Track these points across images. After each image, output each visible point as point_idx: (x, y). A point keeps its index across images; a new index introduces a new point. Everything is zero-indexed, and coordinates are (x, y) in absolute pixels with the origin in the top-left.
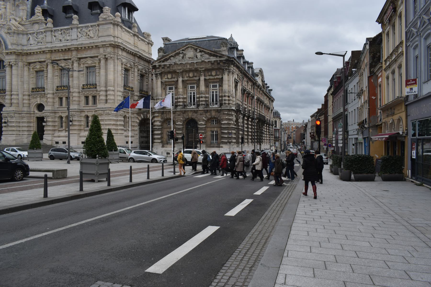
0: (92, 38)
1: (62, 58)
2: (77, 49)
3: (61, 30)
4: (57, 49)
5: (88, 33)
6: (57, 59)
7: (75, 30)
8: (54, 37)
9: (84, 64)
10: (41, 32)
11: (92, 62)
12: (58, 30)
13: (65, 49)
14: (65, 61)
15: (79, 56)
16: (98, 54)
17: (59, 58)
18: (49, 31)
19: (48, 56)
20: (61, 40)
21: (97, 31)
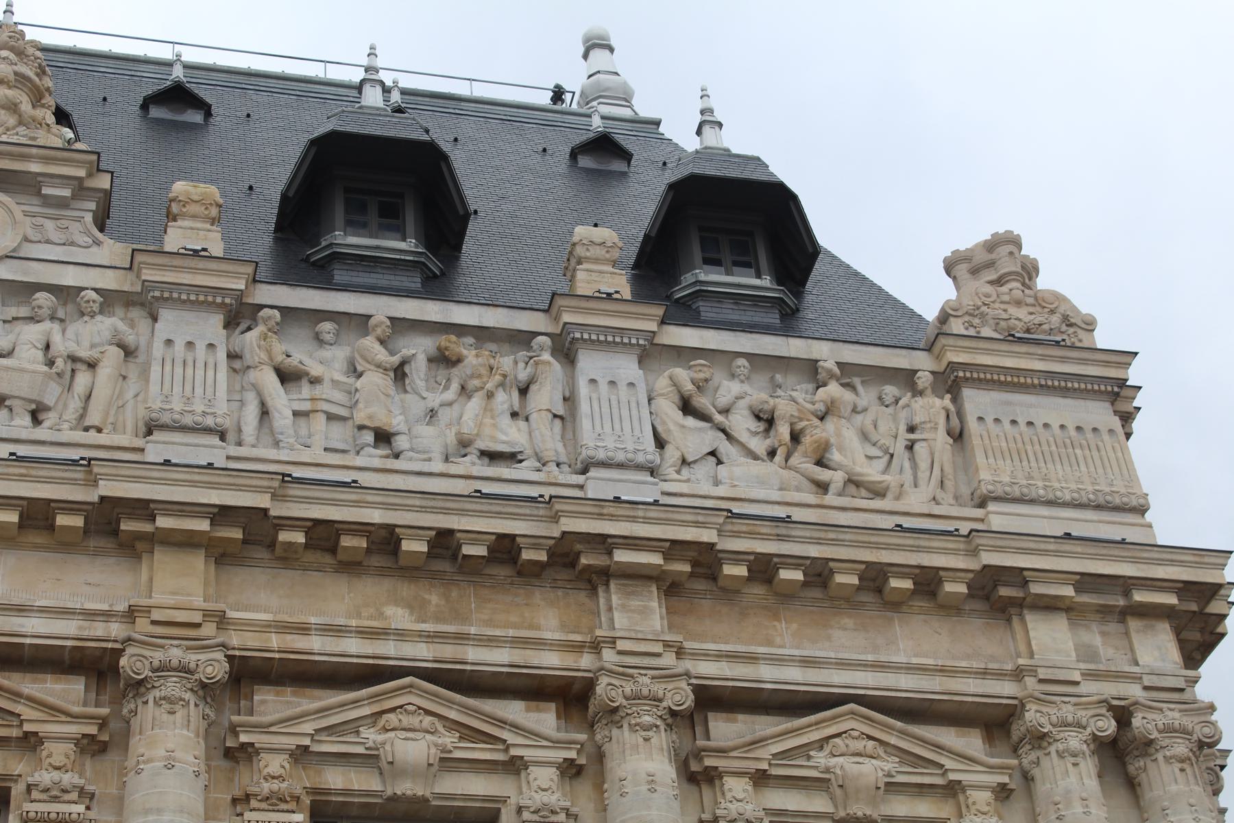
0: (878, 492)
1: (421, 653)
2: (692, 575)
3: (400, 325)
4: (376, 516)
5: (816, 432)
6: (317, 646)
7: (627, 367)
8: (269, 380)
9: (761, 779)
10: (65, 293)
11: (890, 764)
12: (361, 322)
13: (505, 549)
14: (456, 707)
15: (709, 670)
16: (1006, 689)
17: (354, 648)
18: (198, 300)
19: (178, 584)
20: (383, 437)
21: (941, 439)
